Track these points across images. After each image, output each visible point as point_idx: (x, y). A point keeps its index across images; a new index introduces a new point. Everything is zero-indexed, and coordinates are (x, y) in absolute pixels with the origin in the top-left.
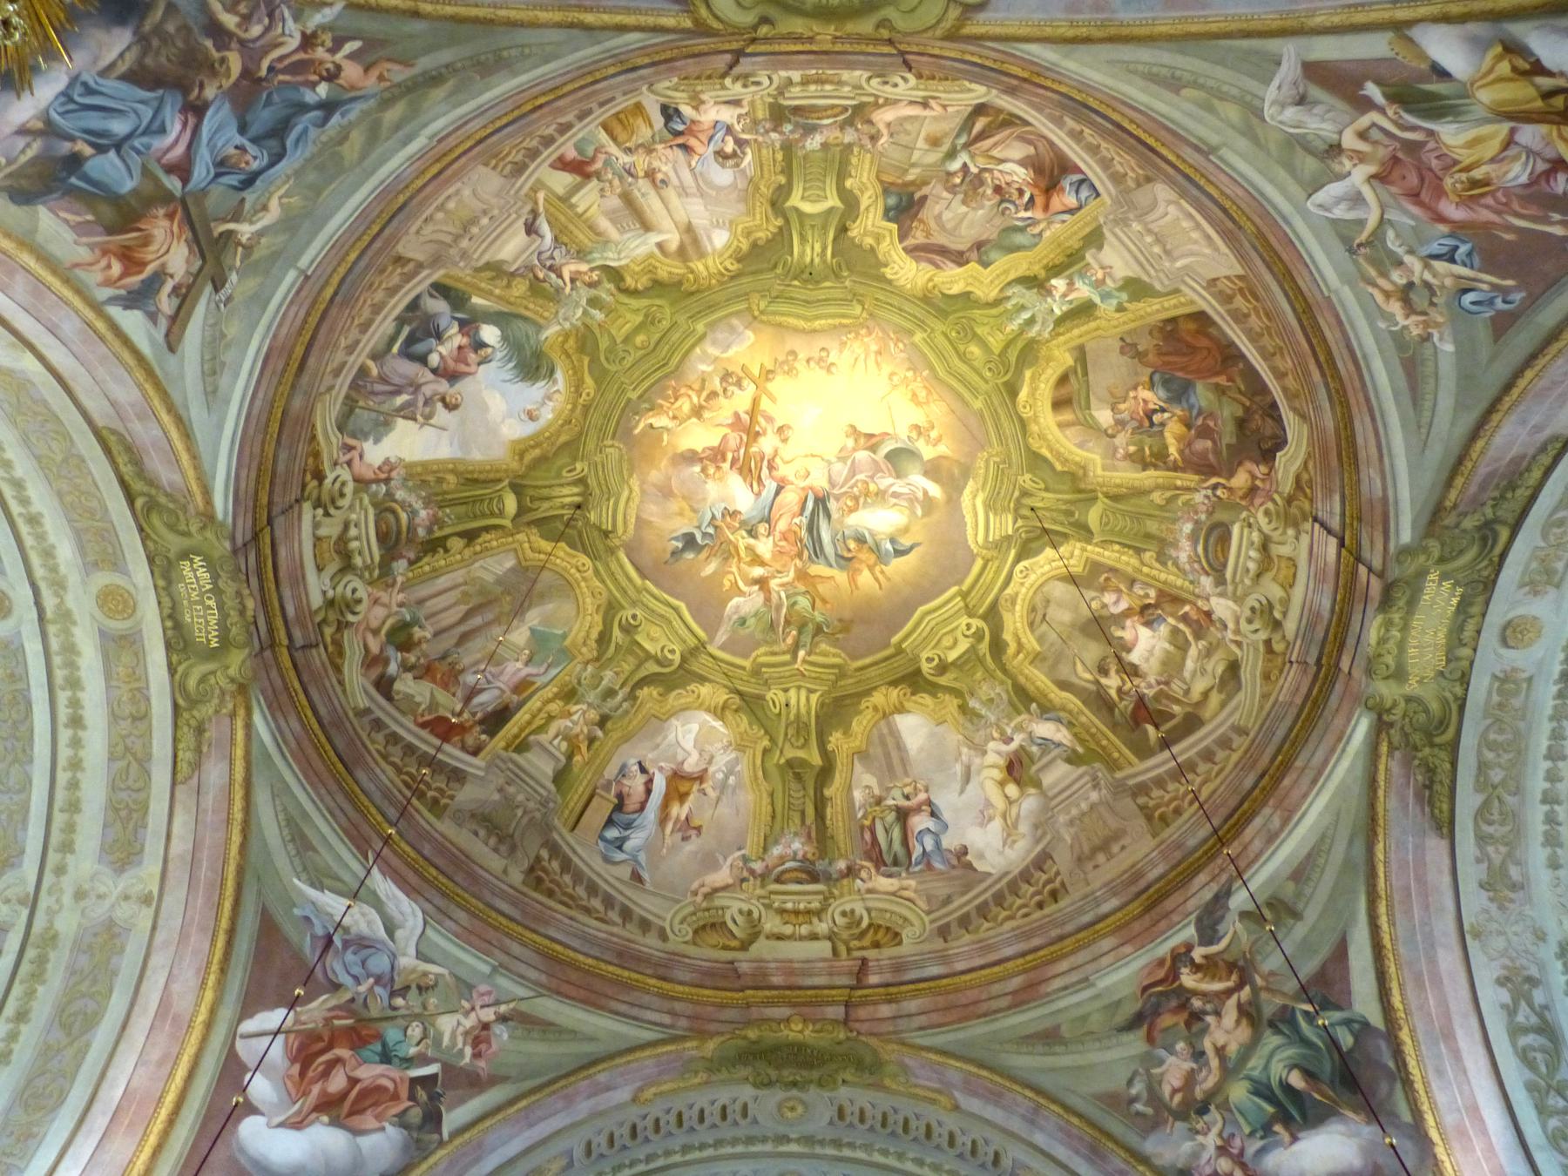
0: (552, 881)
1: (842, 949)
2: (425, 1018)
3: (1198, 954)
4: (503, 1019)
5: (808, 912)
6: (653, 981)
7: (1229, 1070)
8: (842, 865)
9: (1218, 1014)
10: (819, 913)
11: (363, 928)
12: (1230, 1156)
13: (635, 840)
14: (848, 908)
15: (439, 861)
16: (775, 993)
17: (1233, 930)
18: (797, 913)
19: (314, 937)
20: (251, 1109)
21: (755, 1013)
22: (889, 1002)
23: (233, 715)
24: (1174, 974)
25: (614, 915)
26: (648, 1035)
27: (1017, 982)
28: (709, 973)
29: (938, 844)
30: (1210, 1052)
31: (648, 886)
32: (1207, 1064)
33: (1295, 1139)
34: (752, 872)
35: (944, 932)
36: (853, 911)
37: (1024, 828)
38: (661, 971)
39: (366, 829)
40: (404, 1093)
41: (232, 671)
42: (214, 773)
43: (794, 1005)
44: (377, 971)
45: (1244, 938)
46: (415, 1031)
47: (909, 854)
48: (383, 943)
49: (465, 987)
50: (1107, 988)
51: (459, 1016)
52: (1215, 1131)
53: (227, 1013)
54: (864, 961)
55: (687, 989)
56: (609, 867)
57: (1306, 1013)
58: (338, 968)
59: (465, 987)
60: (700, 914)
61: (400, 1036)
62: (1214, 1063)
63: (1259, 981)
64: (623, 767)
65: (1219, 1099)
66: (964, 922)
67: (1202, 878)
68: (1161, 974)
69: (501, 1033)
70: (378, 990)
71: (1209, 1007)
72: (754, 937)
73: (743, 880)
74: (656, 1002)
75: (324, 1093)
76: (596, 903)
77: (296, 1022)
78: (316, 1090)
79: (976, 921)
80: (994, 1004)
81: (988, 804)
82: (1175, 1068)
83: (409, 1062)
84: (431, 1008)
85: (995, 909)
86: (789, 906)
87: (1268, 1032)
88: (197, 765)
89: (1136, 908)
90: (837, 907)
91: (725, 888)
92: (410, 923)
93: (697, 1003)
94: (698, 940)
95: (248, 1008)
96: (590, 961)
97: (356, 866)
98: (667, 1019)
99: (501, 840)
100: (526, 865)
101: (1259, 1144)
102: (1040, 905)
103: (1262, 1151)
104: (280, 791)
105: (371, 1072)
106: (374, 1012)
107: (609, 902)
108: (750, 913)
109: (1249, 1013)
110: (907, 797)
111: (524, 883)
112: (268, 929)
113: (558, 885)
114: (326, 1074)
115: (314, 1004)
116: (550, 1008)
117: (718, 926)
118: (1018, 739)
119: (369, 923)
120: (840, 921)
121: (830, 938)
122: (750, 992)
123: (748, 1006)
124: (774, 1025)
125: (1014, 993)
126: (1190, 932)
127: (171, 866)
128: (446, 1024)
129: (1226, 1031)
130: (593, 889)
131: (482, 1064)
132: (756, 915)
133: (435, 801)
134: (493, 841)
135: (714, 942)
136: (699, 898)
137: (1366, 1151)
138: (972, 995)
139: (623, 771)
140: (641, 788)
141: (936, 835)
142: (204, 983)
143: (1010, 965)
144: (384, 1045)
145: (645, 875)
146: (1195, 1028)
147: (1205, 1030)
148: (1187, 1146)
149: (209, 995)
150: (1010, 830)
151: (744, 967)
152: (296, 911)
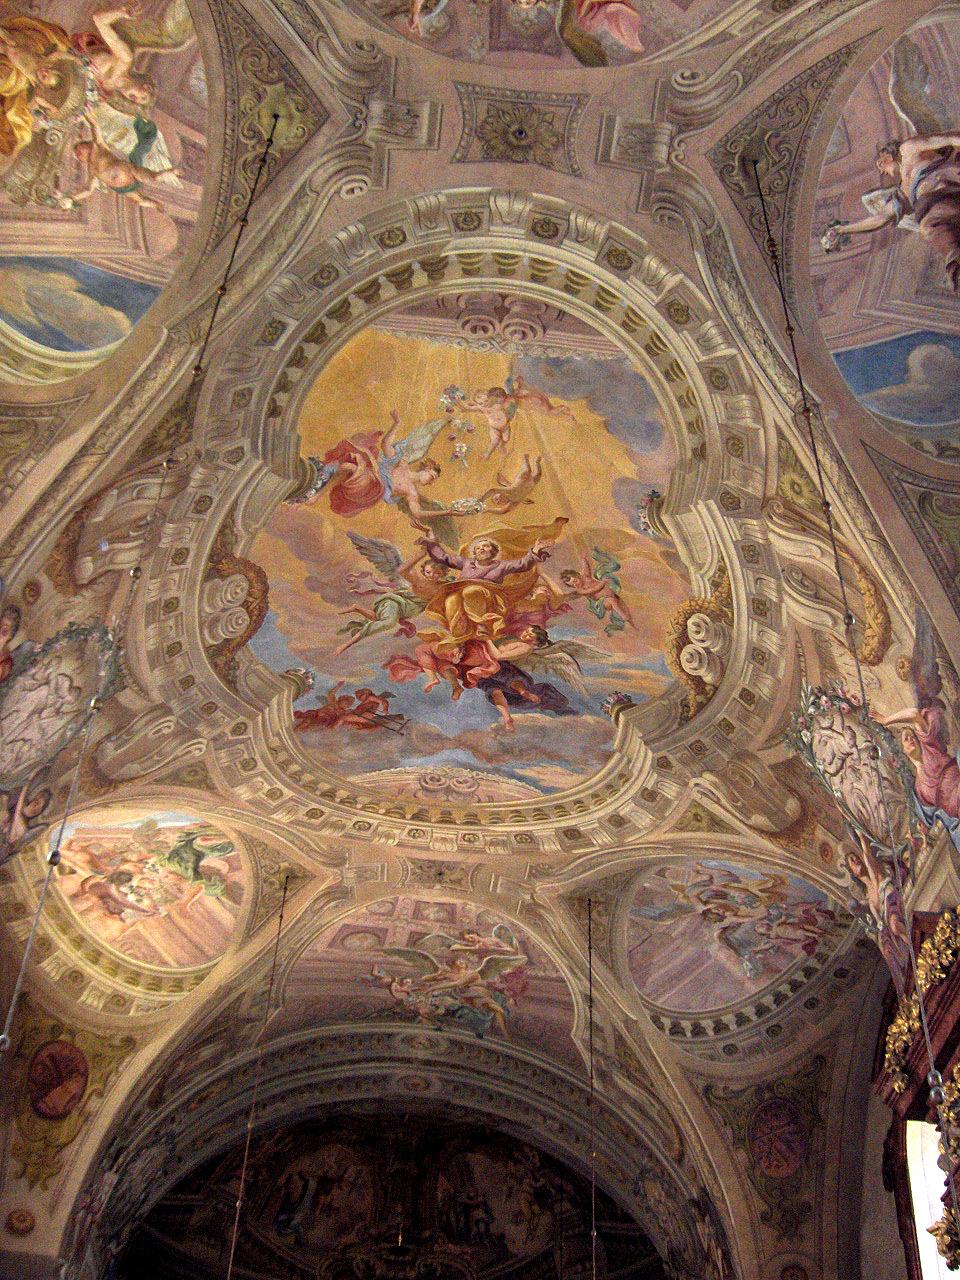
8: (428, 1233)
13: (298, 1219)
29: (487, 1229)
34: (370, 1235)
37: (540, 1231)
47: (469, 1231)
64: (291, 1176)
73: (364, 1241)
81: (520, 1213)
91: (352, 1245)
108: (368, 1261)
110: (471, 1199)
118: (542, 1181)
139: (289, 1179)
140: (300, 1190)
141: (487, 1225)
150: (531, 1232)
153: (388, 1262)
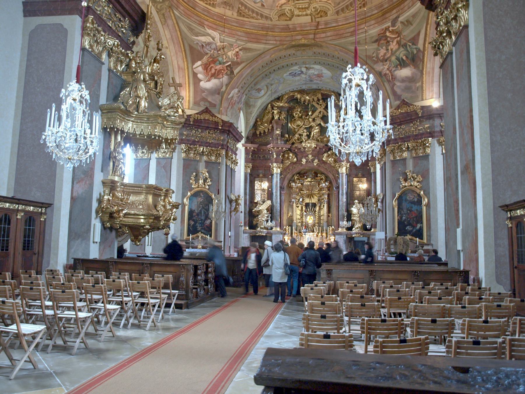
0: (243, 13)
1: (313, 18)
2: (225, 54)
3: (391, 29)
4: (240, 50)
5: (305, 8)
6: (270, 33)
7: (393, 54)
9: (392, 42)
10: (307, 8)
11: (208, 41)
12: (389, 70)
14: (315, 6)
15: (219, 19)
16: (298, 32)
17: (398, 25)
18: (302, 8)
19: (200, 46)
20: (201, 81)
21: (294, 38)
22: (323, 33)
23: (169, 11)
24: (385, 32)
25: (259, 17)
26: (271, 47)
27: (353, 29)
28: (282, 29)
30: (390, 50)
31: (266, 7)
32: (389, 52)
33: (401, 69)
35: (337, 13)
36: (316, 7)
38: (272, 30)
39: (202, 20)
40: (225, 69)
41: (167, 4)
42: (170, 22)
43: (302, 35)
44: (213, 48)
45: (400, 27)
46: (224, 57)
48: (213, 42)
49: (231, 45)
50: (371, 33)
51: (232, 52)
52: (387, 65)
53: (190, 65)
54: (318, 22)
55: (278, 33)
56: (256, 4)
57: (409, 45)
58: (206, 50)
59: (231, 45)
60: (279, 12)
61: (222, 59)
62: (390, 52)
63: (402, 37)
65: (390, 59)
66: (343, 10)
67: (395, 11)
68: (382, 32)
69: (241, 53)
70: (215, 51)
71: (391, 40)
72: (293, 16)
74: (272, 38)
75: (211, 74)
76: (255, 15)
77: (202, 63)
78: (210, 73)
79: (346, 10)
80: (346, 35)
82: (382, 52)
83: (224, 63)
84: (226, 52)
85: (350, 7)
86: (300, 7)
87: (401, 47)
88: (166, 21)
89: (380, 14)
90: (312, 6)
91: (285, 4)
92: (217, 36)
93: (281, 37)
94: (280, 20)
95: (193, 64)
96: (256, 31)
97: (203, 30)
98: (275, 42)
99: (229, 6)
100: (237, 11)
101: (395, 69)
102: (360, 8)
103: (395, 70)
104: (184, 22)
105: (218, 67)
106: (215, 56)
107: (257, 14)
108: (291, 10)
109: (398, 43)
111: (237, 16)
112: (191, 48)
113: (245, 13)
114: (211, 70)
115: (204, 58)
116: (249, 45)
117: (283, 14)
119: (209, 39)
120: (313, 10)
121: (310, 15)
122: (292, 33)
123: (292, 36)
124: (298, 41)
125: (351, 32)
126: (390, 24)
127: (168, 41)
128: (230, 54)
129: (393, 46)
130: (253, 11)
131: (238, 60)
132: (292, 10)
133: (213, 4)
134: (228, 7)
135: (283, 19)
136: (278, 8)
137: (413, 74)
138: (342, 32)
142: (184, 62)
143: (351, 24)
144: (219, 61)
145: (265, 4)
146: (387, 44)
147: (389, 45)
148: (382, 68)
149: (186, 63)
151: (291, 26)
152: (195, 43)
153: (299, 8)
